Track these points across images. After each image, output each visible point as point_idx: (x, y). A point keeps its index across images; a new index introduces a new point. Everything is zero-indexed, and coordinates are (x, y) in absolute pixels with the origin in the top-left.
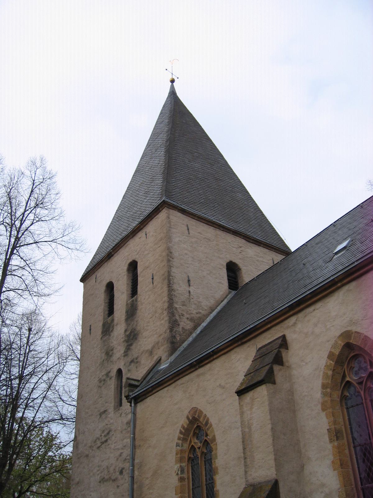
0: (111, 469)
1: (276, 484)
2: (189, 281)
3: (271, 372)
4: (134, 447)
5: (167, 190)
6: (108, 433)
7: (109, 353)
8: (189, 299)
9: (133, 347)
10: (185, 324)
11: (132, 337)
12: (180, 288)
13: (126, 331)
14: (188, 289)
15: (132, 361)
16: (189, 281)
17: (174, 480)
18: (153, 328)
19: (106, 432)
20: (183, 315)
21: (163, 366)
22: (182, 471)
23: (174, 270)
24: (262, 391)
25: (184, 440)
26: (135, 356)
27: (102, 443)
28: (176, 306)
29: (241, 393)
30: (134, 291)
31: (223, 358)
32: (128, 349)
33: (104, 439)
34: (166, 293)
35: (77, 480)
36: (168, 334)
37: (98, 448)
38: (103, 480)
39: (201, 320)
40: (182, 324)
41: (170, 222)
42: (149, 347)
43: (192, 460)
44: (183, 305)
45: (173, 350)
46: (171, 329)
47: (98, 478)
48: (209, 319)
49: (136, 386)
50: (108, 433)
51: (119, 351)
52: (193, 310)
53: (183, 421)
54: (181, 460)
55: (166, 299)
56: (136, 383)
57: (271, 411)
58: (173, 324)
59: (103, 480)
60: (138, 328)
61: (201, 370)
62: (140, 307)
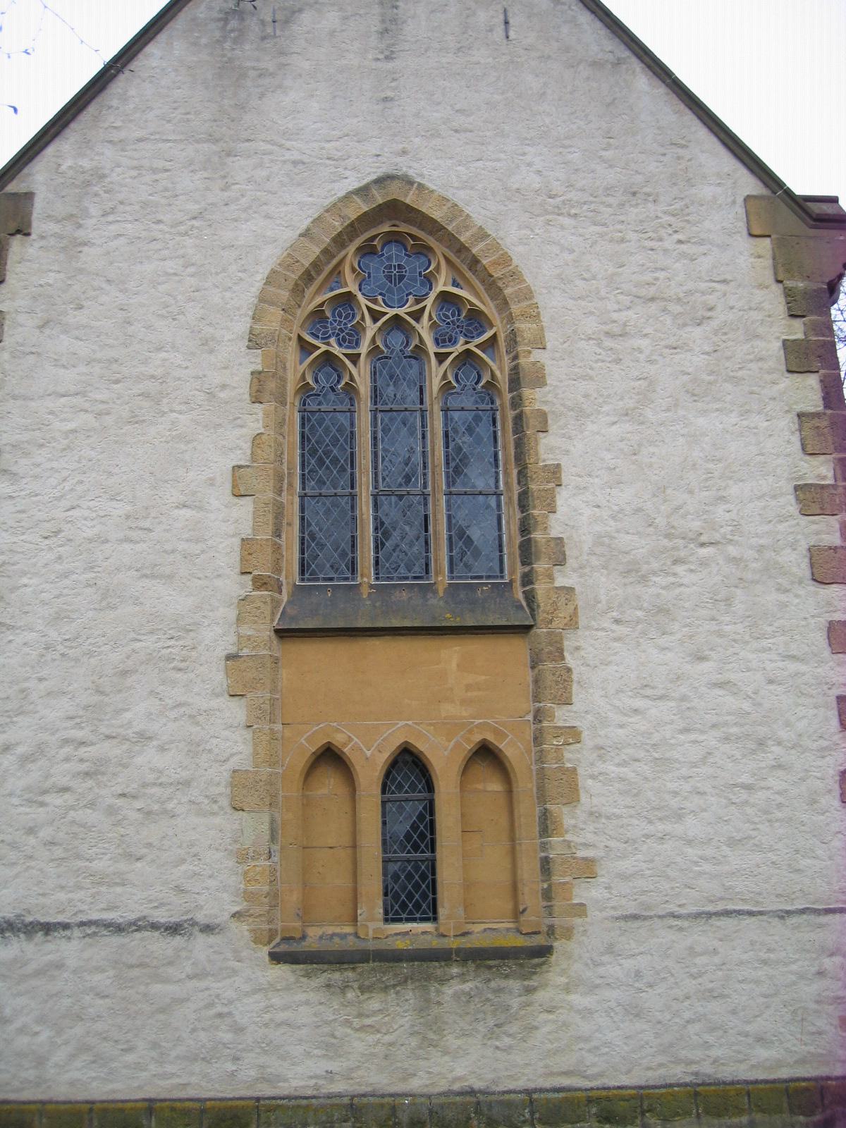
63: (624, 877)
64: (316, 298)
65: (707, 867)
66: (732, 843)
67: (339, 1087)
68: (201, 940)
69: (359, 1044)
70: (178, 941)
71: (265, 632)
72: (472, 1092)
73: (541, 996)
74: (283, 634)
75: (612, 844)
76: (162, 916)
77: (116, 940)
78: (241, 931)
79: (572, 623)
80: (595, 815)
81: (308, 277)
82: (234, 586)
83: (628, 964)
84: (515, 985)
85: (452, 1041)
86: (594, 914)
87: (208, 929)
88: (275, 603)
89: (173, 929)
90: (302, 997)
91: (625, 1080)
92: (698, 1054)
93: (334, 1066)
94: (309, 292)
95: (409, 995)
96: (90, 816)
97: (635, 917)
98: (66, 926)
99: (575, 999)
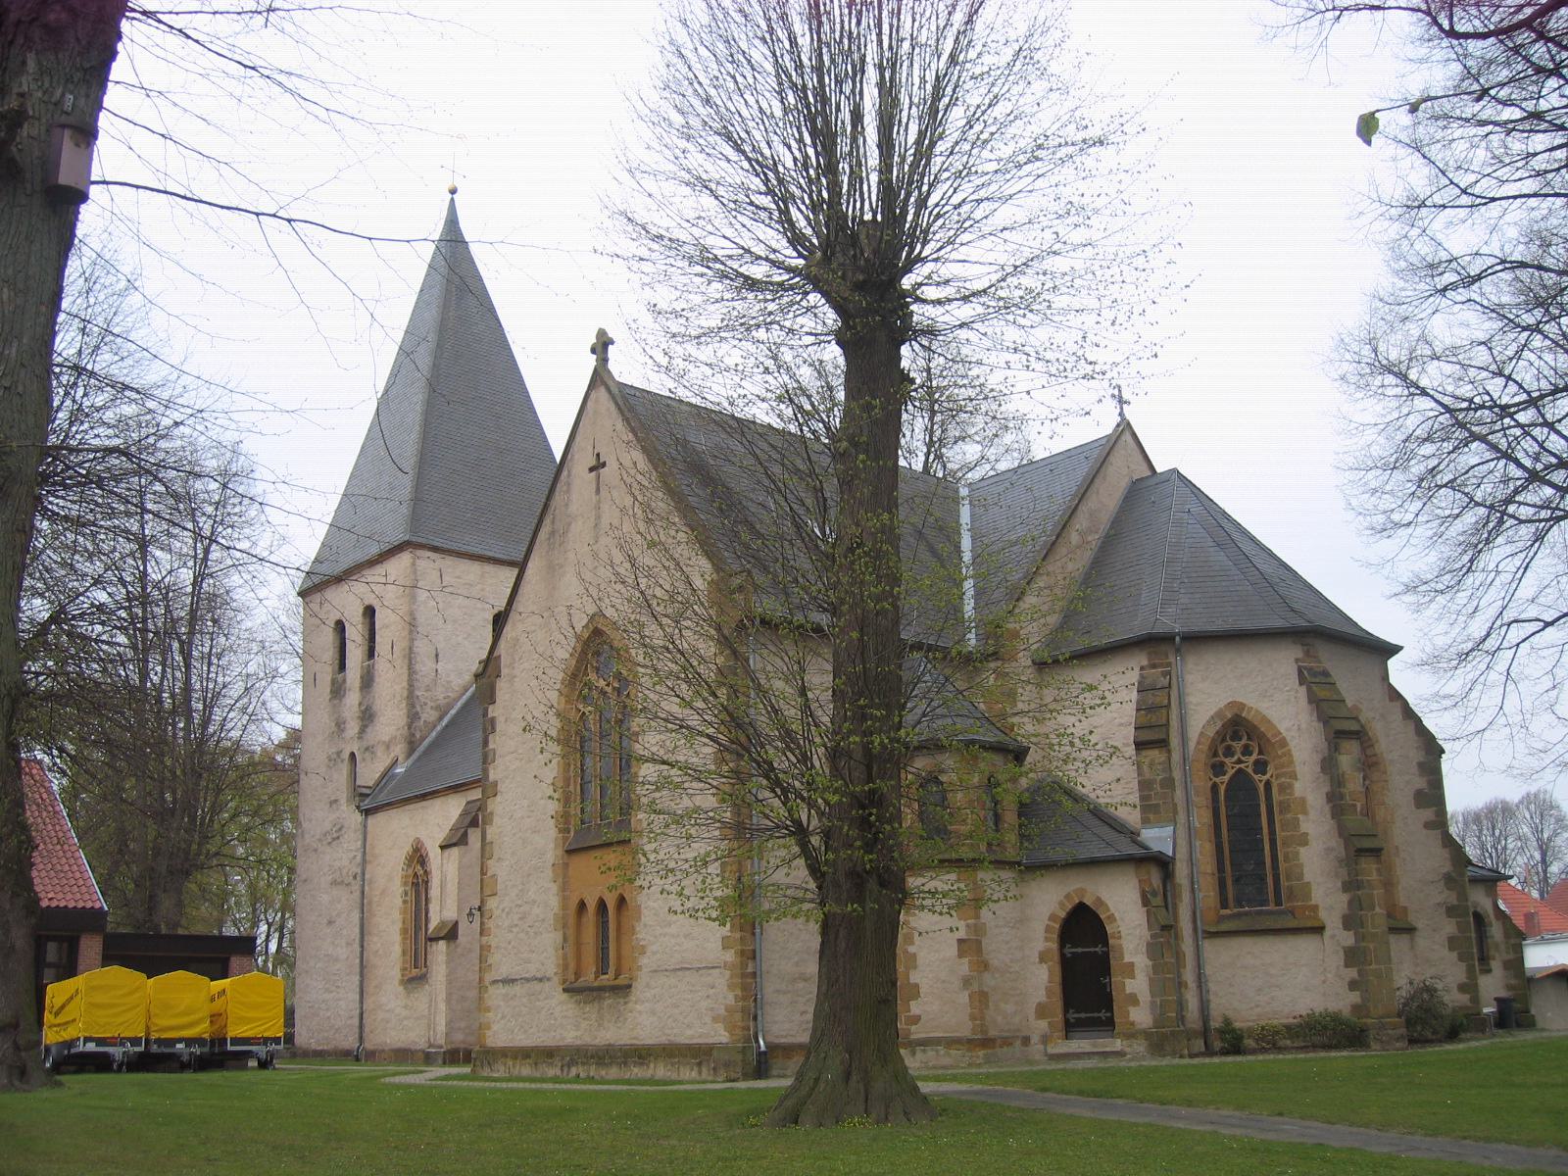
0: (345, 871)
1: (457, 922)
2: (437, 655)
3: (465, 834)
4: (364, 862)
5: (415, 519)
6: (340, 829)
7: (340, 725)
8: (435, 681)
9: (369, 730)
10: (428, 715)
11: (367, 716)
12: (425, 666)
13: (360, 704)
15: (367, 749)
16: (437, 655)
17: (399, 902)
18: (391, 721)
19: (338, 827)
20: (426, 704)
21: (399, 770)
22: (406, 894)
23: (416, 643)
24: (455, 851)
25: (409, 866)
26: (371, 743)
27: (334, 839)
28: (418, 693)
29: (443, 847)
30: (371, 653)
31: (442, 798)
32: (363, 730)
33: (335, 835)
34: (405, 677)
35: (304, 877)
36: (405, 731)
37: (330, 843)
38: (334, 883)
39: (450, 706)
40: (424, 717)
41: (415, 572)
42: (386, 738)
43: (415, 885)
44: (427, 691)
45: (411, 751)
48: (459, 704)
49: (368, 795)
50: (340, 829)
51: (352, 728)
52: (440, 694)
53: (408, 848)
54: (405, 884)
55: (405, 684)
56: (368, 791)
57: (459, 868)
58: (413, 717)
59: (334, 883)
60: (374, 708)
61: (424, 803)
62: (377, 680)
63: (654, 953)
65: (677, 948)
66: (686, 936)
67: (579, 1042)
68: (547, 984)
69: (584, 1025)
71: (560, 852)
72: (609, 1045)
73: (630, 1005)
74: (570, 852)
75: (651, 939)
76: (539, 975)
78: (556, 979)
80: (645, 925)
81: (574, 676)
82: (553, 833)
83: (653, 992)
84: (622, 1001)
86: (645, 970)
87: (548, 979)
88: (565, 839)
89: (541, 980)
90: (570, 1006)
91: (650, 1042)
92: (669, 1032)
93: (579, 1033)
95: (596, 1004)
96: (522, 935)
97: (655, 971)
98: (516, 980)
99: (638, 1007)
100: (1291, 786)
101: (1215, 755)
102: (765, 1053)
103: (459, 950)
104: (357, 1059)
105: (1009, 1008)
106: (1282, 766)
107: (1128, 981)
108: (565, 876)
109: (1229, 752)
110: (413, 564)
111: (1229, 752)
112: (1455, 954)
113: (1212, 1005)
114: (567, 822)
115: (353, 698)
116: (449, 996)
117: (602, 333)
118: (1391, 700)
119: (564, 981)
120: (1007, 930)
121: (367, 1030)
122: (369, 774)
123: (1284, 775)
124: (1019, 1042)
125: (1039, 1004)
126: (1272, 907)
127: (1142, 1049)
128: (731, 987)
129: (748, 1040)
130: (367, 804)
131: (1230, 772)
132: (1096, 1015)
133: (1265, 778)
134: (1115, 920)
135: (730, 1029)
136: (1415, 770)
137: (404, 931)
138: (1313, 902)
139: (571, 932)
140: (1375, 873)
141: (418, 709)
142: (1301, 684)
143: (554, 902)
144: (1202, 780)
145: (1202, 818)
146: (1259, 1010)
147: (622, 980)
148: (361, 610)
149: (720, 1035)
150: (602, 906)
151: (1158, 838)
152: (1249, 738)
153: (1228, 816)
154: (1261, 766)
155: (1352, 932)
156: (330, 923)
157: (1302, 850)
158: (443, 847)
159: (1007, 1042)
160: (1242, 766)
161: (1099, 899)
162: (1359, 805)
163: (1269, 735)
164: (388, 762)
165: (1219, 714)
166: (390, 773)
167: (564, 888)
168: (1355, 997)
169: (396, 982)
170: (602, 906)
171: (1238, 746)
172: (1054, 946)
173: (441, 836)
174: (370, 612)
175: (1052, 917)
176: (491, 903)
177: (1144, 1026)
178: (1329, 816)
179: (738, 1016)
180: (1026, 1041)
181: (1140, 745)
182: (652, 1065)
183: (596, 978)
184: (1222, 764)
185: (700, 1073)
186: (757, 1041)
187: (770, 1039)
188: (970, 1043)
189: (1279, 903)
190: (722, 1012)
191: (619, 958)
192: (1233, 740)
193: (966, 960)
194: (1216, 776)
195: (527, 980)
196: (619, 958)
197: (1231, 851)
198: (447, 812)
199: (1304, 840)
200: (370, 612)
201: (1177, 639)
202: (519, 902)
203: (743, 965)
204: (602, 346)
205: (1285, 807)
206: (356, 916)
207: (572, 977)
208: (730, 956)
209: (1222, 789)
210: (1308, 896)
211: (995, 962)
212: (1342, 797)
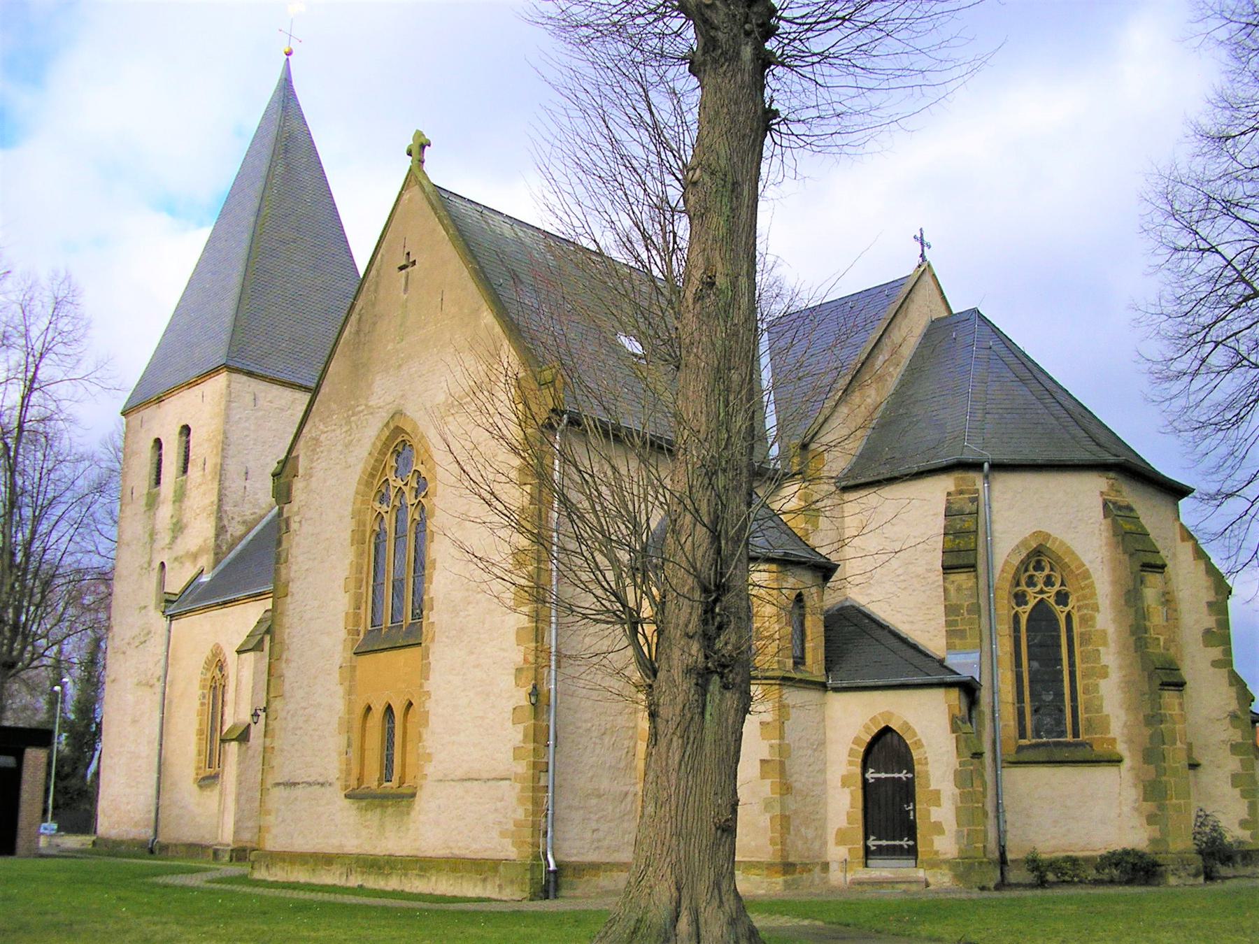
7: (152, 535)
9: (179, 541)
10: (236, 529)
11: (178, 528)
14: (243, 484)
15: (176, 559)
17: (197, 704)
18: (201, 532)
21: (205, 578)
23: (229, 461)
24: (250, 655)
29: (239, 652)
35: (112, 677)
36: (212, 542)
38: (139, 684)
40: (230, 530)
42: (194, 549)
45: (217, 561)
46: (217, 536)
47: (136, 681)
51: (164, 538)
52: (248, 512)
53: (208, 653)
54: (204, 687)
55: (215, 498)
56: (174, 598)
58: (220, 530)
59: (139, 684)
64: (377, 483)
67: (358, 851)
69: (364, 832)
70: (323, 789)
71: (349, 654)
76: (321, 780)
77: (309, 789)
78: (338, 785)
79: (433, 639)
81: (372, 476)
82: (343, 634)
85: (387, 834)
86: (429, 778)
89: (323, 785)
94: (375, 482)
100: (1092, 618)
101: (1018, 584)
102: (554, 872)
103: (250, 752)
104: (152, 851)
105: (810, 833)
106: (1085, 597)
107: (933, 809)
108: (352, 679)
109: (1031, 582)
110: (229, 386)
111: (1031, 582)
112: (1237, 791)
113: (1009, 836)
114: (357, 623)
115: (165, 512)
116: (239, 795)
117: (419, 134)
118: (1183, 540)
119: (347, 787)
120: (810, 752)
121: (161, 824)
122: (176, 582)
123: (1086, 606)
124: (818, 869)
125: (840, 829)
126: (1069, 738)
127: (946, 879)
128: (521, 800)
129: (536, 857)
130: (172, 609)
131: (1032, 603)
132: (897, 843)
133: (1067, 609)
134: (922, 746)
135: (518, 844)
136: (1205, 609)
137: (200, 732)
138: (1111, 735)
139: (356, 736)
140: (1177, 707)
141: (226, 522)
142: (1105, 517)
143: (340, 705)
144: (1004, 607)
145: (1004, 647)
146: (1053, 842)
147: (404, 790)
148: (178, 429)
149: (509, 851)
150: (389, 709)
151: (965, 663)
152: (1052, 569)
153: (1029, 647)
154: (1062, 598)
155: (1152, 767)
156: (134, 722)
157: (1102, 683)
158: (239, 652)
159: (807, 868)
160: (1044, 596)
161: (906, 723)
162: (1162, 638)
163: (1073, 567)
164: (194, 572)
165: (1024, 543)
166: (195, 583)
167: (350, 692)
168: (1154, 831)
169: (191, 781)
170: (389, 709)
171: (1040, 576)
172: (858, 770)
173: (239, 641)
174: (186, 430)
175: (856, 741)
176: (277, 704)
177: (949, 856)
178: (1132, 649)
179: (528, 832)
180: (825, 866)
181: (947, 569)
182: (434, 879)
183: (380, 784)
184: (1024, 594)
185: (485, 889)
186: (546, 859)
187: (561, 857)
188: (770, 866)
189: (1076, 734)
190: (511, 827)
191: (404, 766)
192: (1036, 569)
193: (768, 781)
194: (1018, 605)
195: (310, 784)
196: (404, 766)
197: (1031, 682)
198: (247, 616)
199: (1104, 674)
200: (186, 430)
201: (986, 465)
202: (303, 704)
203: (536, 779)
204: (420, 147)
205: (1086, 639)
206: (157, 715)
207: (354, 783)
208: (522, 768)
209: (1024, 619)
210: (1106, 729)
211: (797, 785)
212: (1146, 630)
